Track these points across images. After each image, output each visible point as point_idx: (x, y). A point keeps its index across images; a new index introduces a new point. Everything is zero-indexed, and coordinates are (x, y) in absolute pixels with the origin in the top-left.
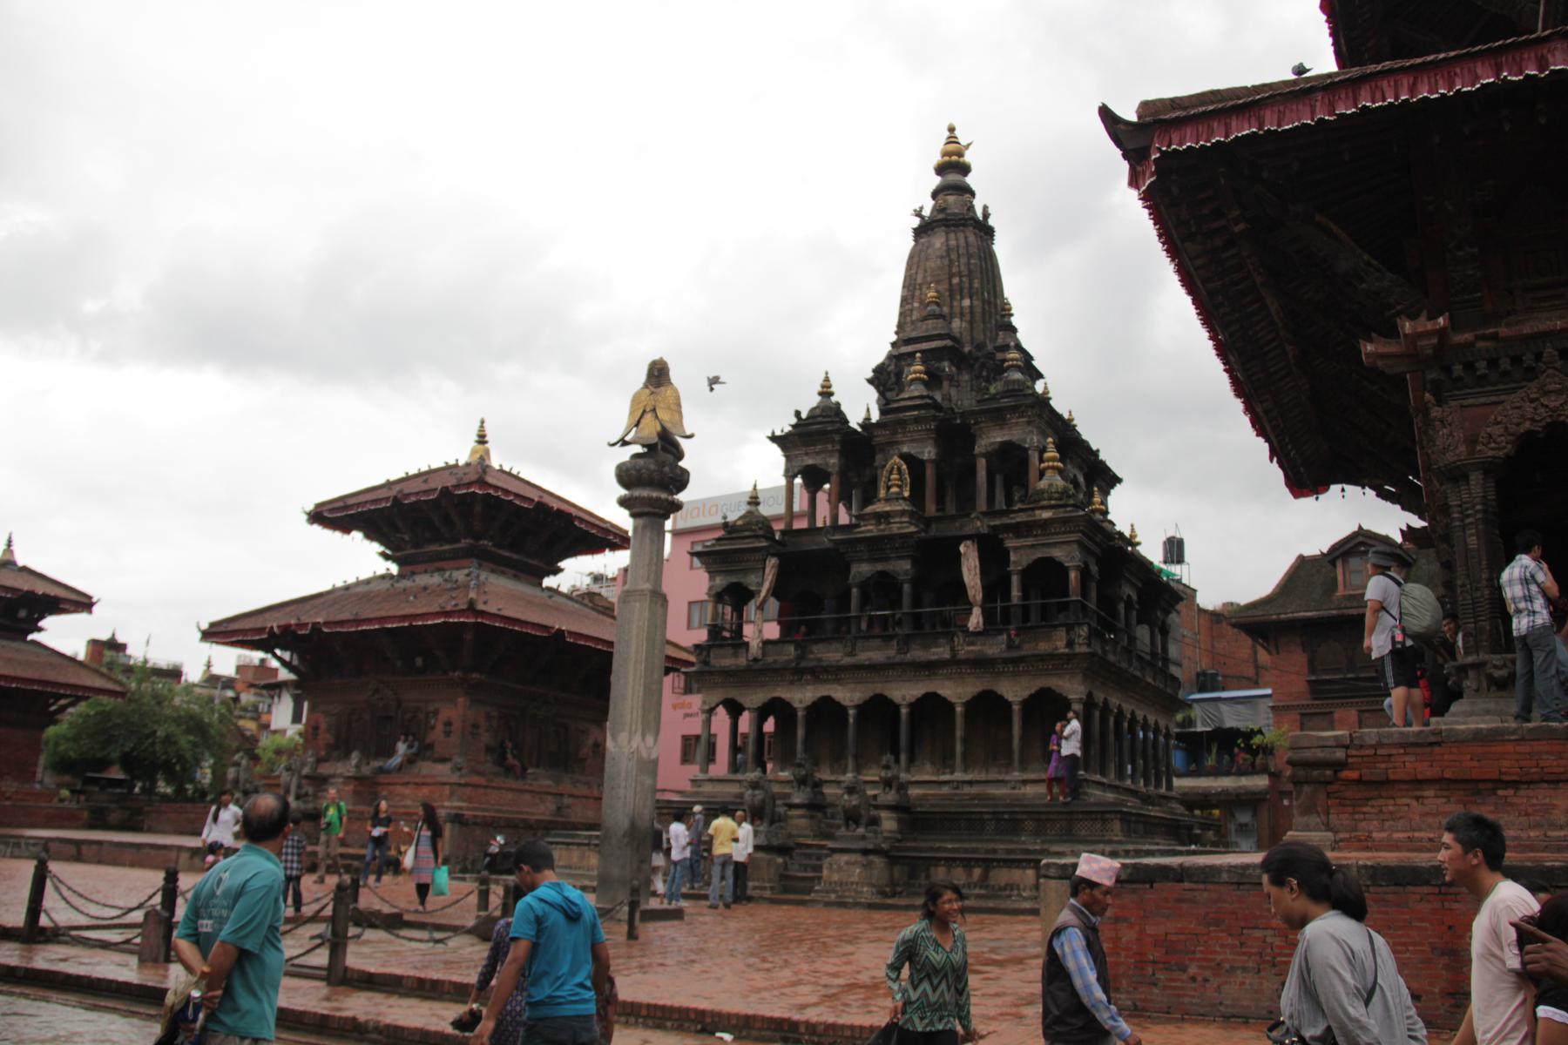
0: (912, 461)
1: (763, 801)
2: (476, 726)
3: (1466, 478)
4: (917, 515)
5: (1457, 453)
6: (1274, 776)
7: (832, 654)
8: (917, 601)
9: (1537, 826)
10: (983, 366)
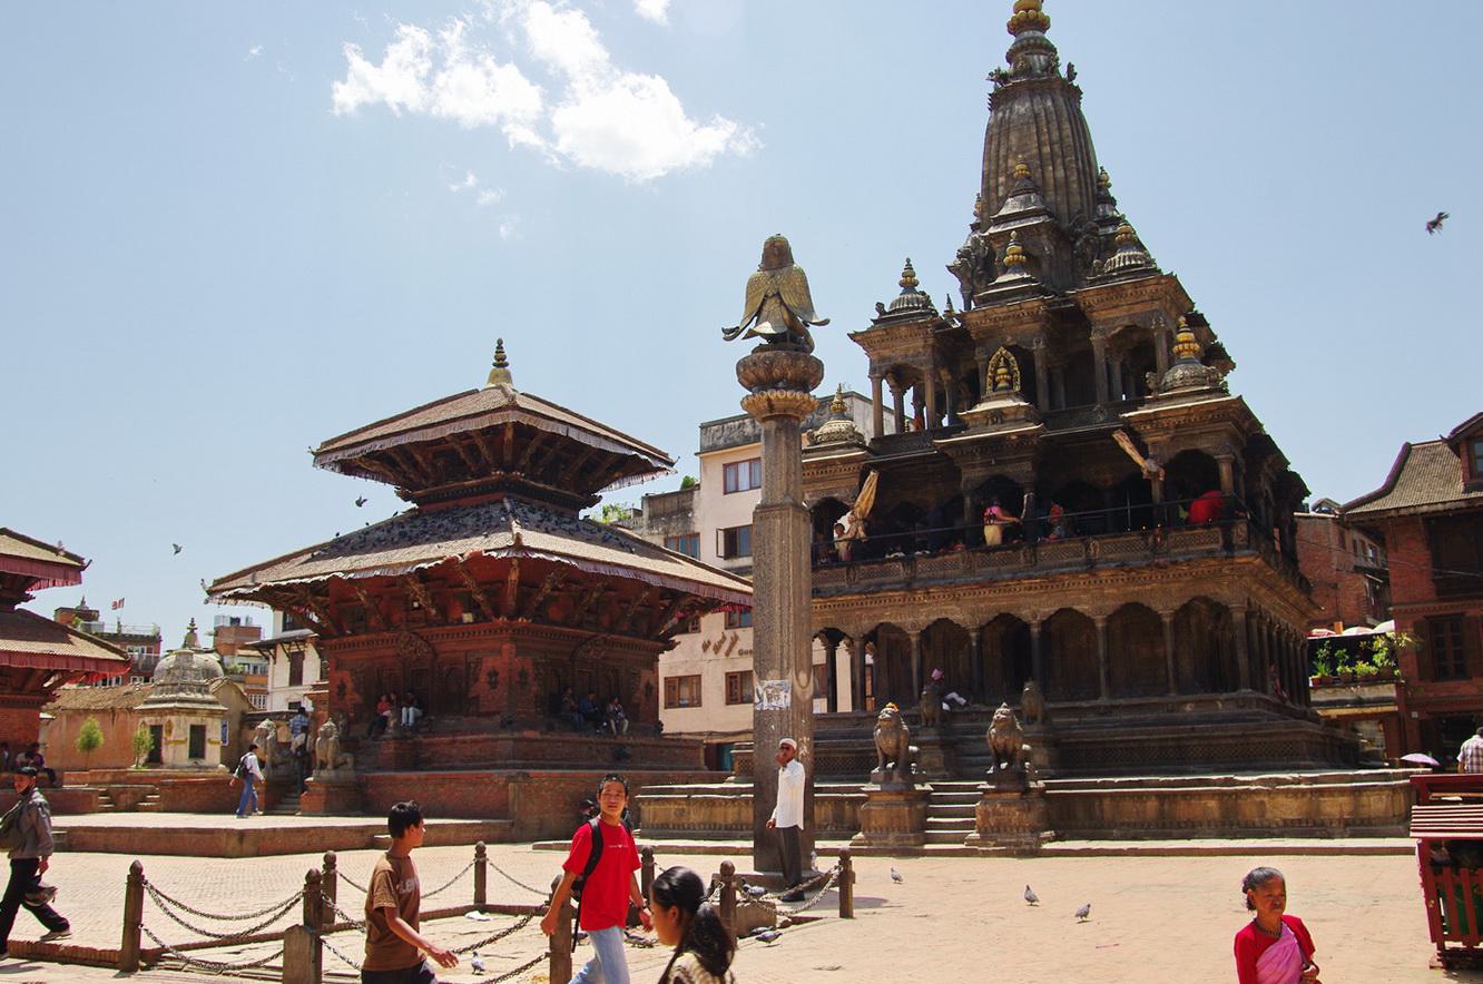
2: (523, 674)
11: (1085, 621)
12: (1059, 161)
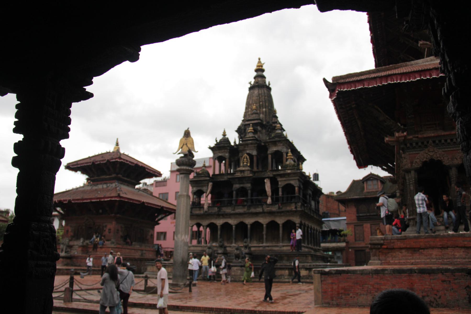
0: (251, 156)
1: (212, 252)
2: (118, 230)
3: (410, 172)
4: (252, 171)
5: (408, 166)
6: (347, 243)
7: (228, 210)
8: (252, 196)
9: (429, 259)
10: (269, 128)
11: (261, 225)
12: (264, 106)
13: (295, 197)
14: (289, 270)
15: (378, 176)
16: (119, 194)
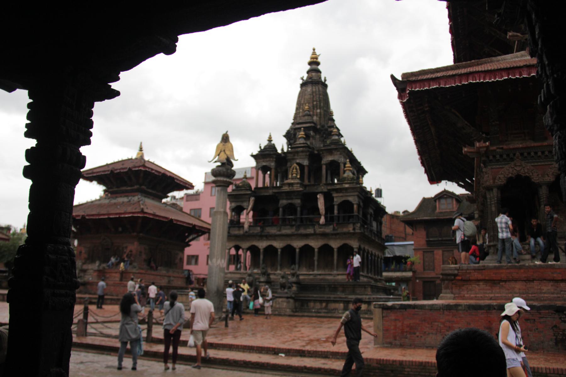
0: (301, 166)
1: (252, 281)
2: (141, 252)
3: (492, 190)
4: (302, 185)
5: (490, 183)
6: (414, 272)
7: (273, 231)
8: (302, 214)
10: (324, 133)
13: (353, 216)
14: (344, 303)
15: (453, 194)
16: (142, 209)
